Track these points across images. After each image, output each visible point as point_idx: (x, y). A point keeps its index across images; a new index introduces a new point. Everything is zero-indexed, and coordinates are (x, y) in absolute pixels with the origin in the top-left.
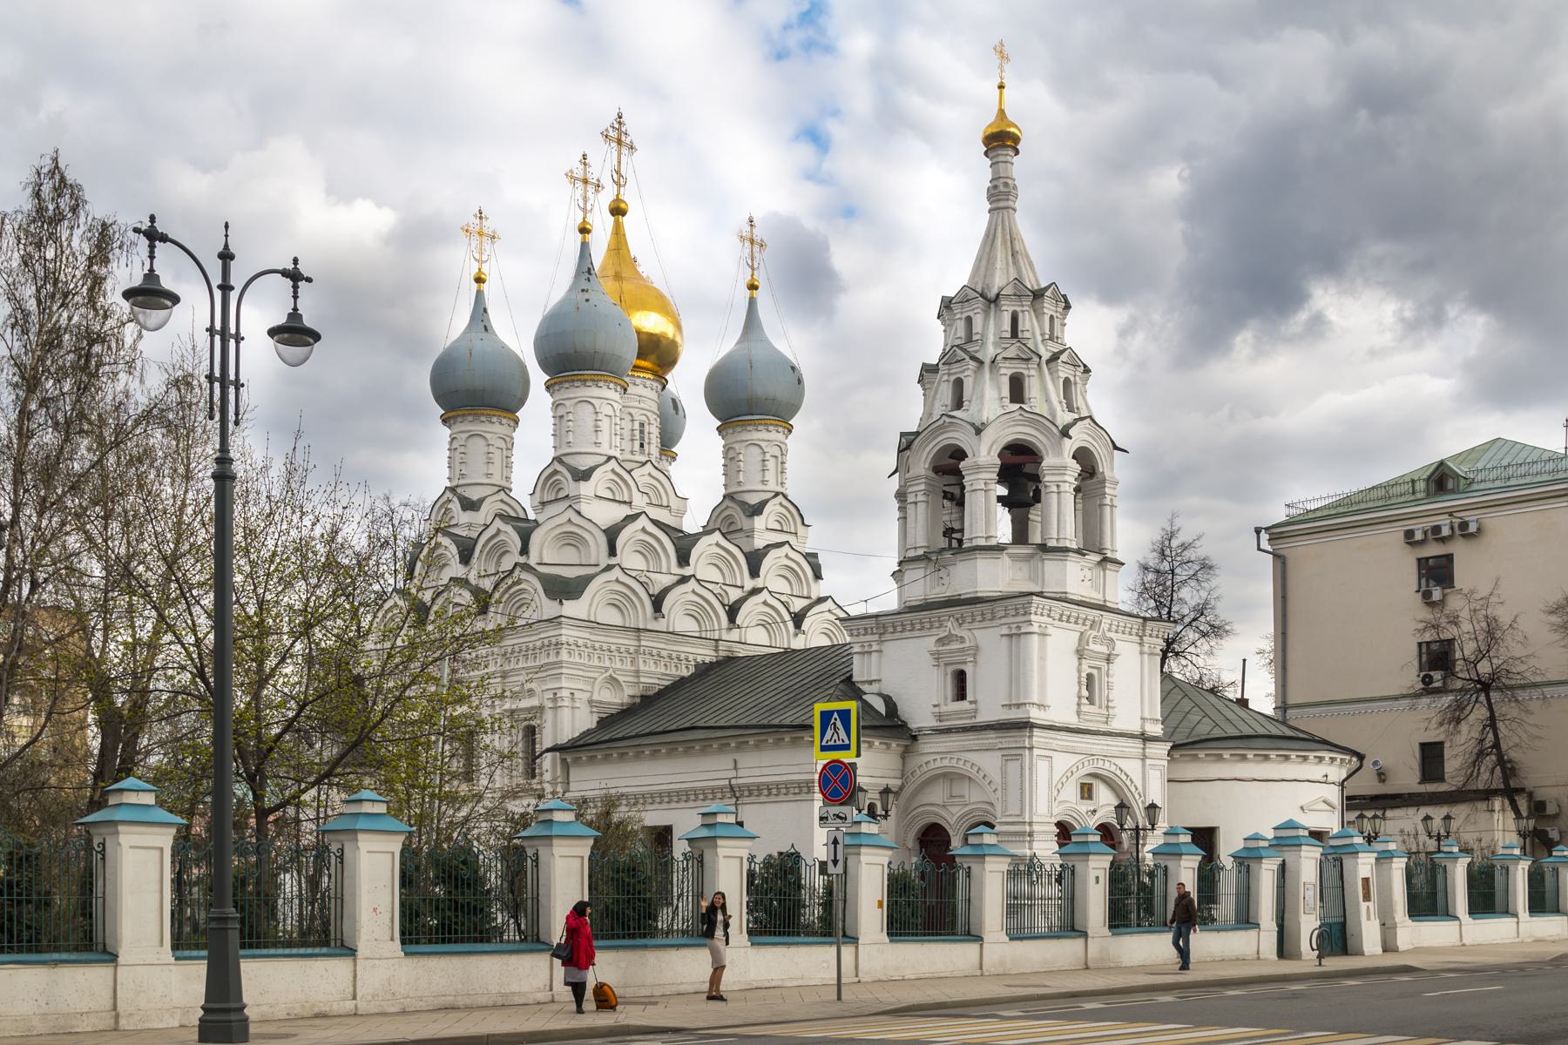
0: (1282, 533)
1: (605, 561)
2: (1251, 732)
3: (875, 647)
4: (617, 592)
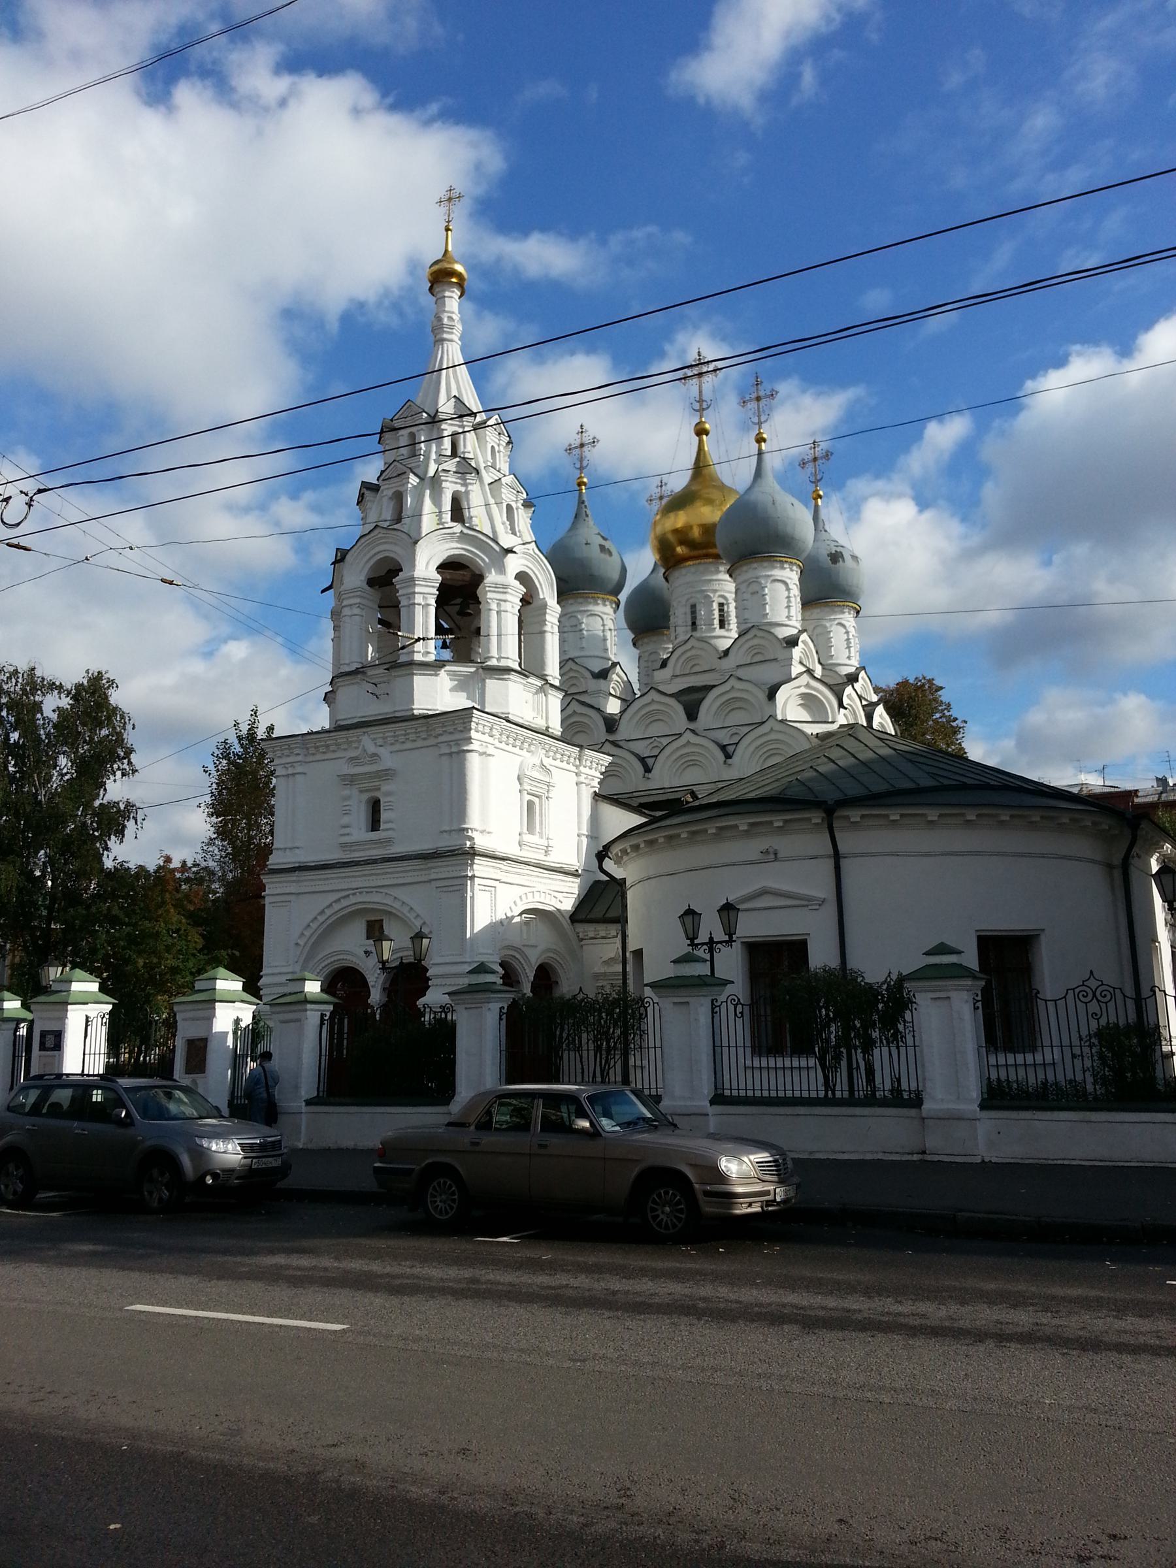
3: (299, 769)
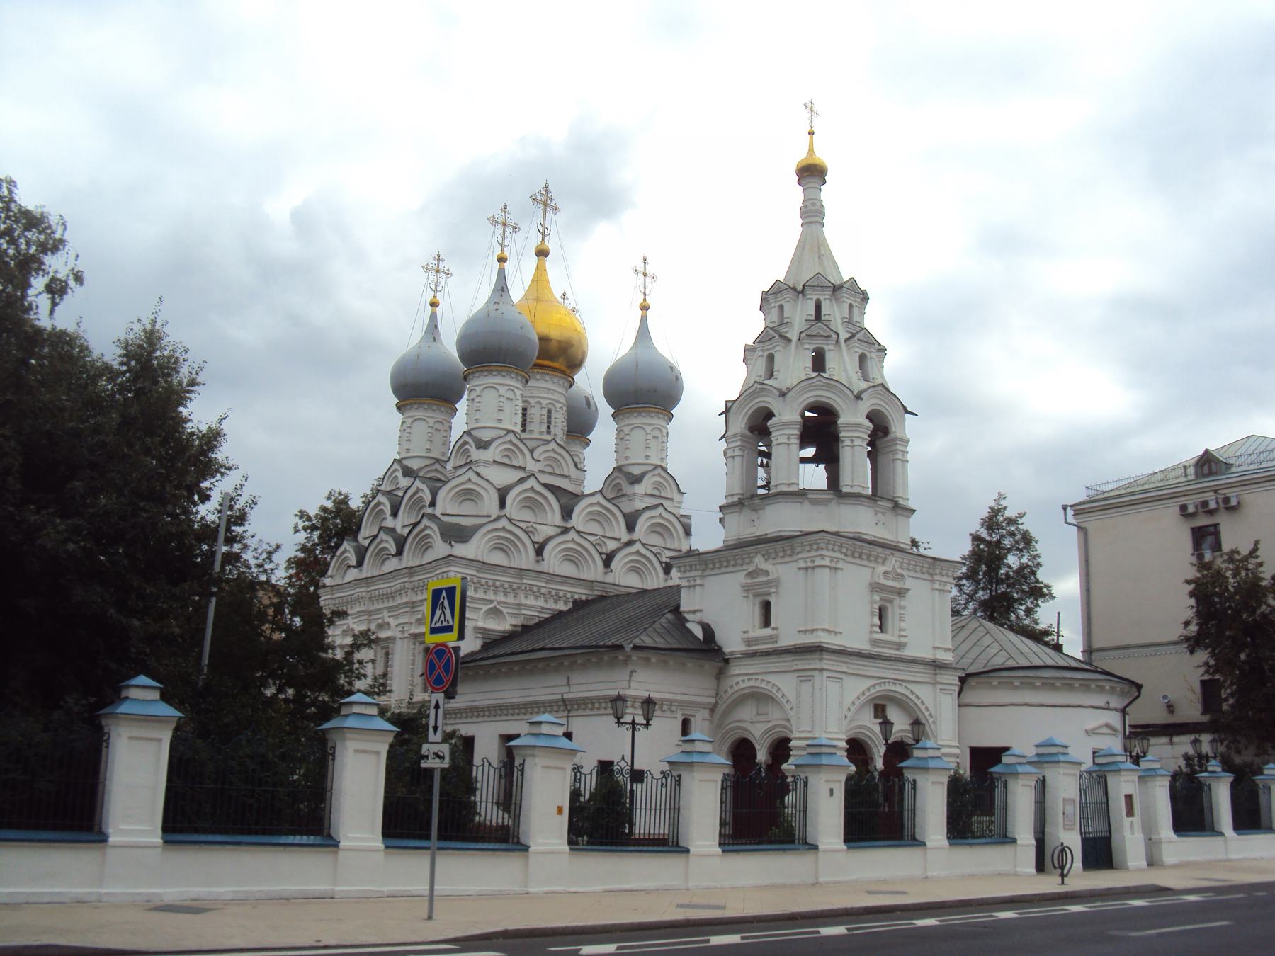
0: (1084, 509)
1: (495, 511)
2: (1042, 664)
3: (698, 582)
4: (503, 538)
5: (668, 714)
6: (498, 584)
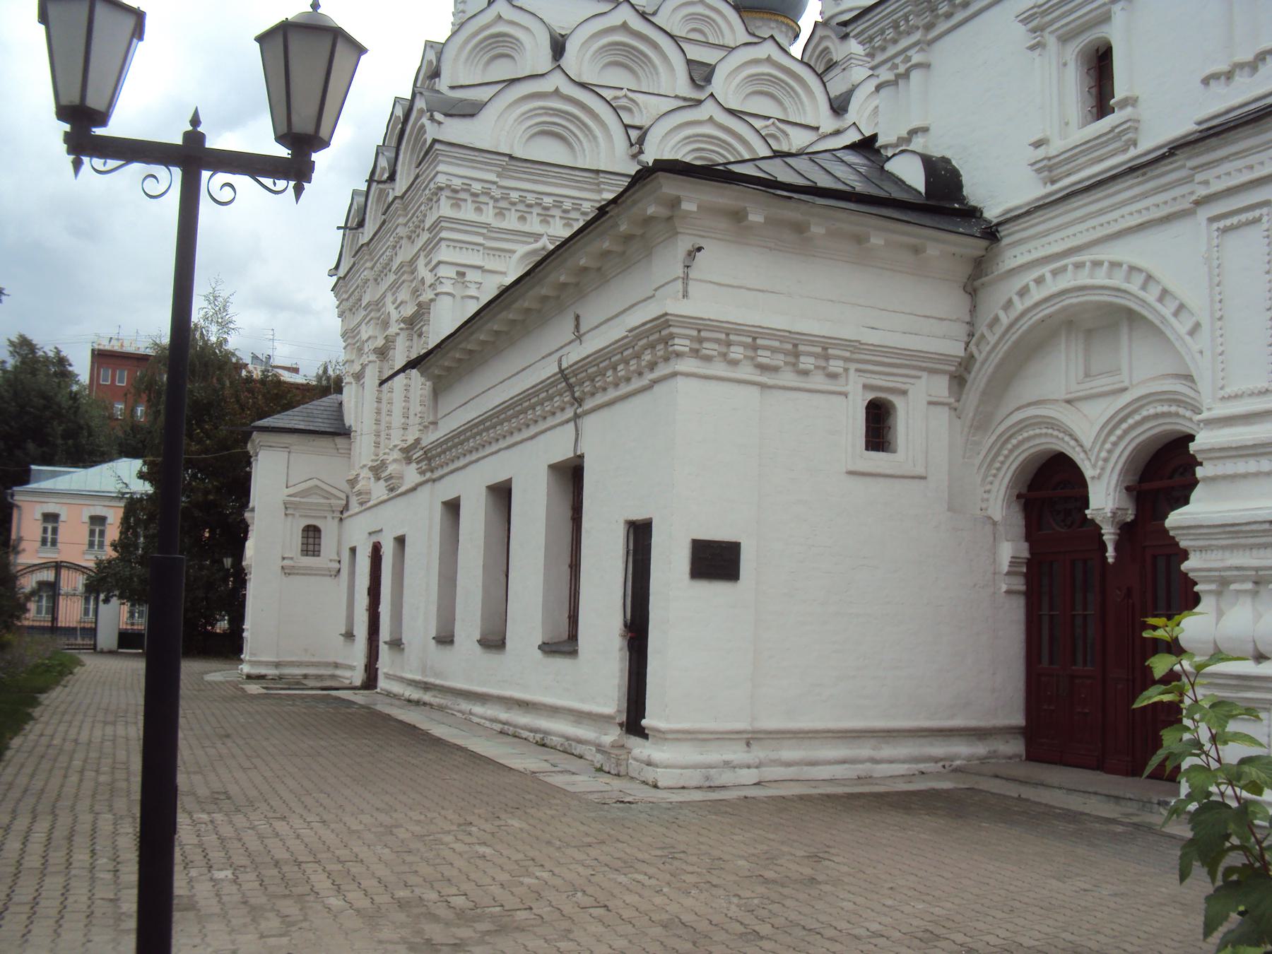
3: (916, 58)
4: (558, 113)
5: (818, 381)
6: (548, 201)
